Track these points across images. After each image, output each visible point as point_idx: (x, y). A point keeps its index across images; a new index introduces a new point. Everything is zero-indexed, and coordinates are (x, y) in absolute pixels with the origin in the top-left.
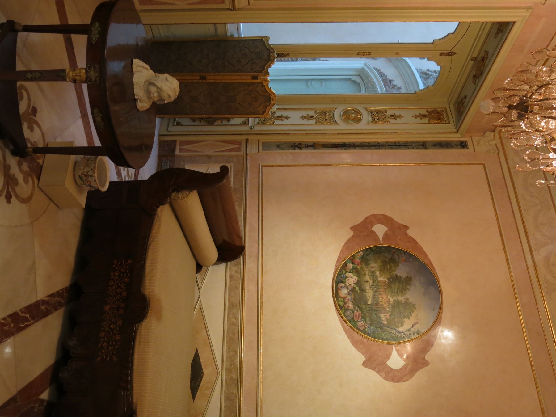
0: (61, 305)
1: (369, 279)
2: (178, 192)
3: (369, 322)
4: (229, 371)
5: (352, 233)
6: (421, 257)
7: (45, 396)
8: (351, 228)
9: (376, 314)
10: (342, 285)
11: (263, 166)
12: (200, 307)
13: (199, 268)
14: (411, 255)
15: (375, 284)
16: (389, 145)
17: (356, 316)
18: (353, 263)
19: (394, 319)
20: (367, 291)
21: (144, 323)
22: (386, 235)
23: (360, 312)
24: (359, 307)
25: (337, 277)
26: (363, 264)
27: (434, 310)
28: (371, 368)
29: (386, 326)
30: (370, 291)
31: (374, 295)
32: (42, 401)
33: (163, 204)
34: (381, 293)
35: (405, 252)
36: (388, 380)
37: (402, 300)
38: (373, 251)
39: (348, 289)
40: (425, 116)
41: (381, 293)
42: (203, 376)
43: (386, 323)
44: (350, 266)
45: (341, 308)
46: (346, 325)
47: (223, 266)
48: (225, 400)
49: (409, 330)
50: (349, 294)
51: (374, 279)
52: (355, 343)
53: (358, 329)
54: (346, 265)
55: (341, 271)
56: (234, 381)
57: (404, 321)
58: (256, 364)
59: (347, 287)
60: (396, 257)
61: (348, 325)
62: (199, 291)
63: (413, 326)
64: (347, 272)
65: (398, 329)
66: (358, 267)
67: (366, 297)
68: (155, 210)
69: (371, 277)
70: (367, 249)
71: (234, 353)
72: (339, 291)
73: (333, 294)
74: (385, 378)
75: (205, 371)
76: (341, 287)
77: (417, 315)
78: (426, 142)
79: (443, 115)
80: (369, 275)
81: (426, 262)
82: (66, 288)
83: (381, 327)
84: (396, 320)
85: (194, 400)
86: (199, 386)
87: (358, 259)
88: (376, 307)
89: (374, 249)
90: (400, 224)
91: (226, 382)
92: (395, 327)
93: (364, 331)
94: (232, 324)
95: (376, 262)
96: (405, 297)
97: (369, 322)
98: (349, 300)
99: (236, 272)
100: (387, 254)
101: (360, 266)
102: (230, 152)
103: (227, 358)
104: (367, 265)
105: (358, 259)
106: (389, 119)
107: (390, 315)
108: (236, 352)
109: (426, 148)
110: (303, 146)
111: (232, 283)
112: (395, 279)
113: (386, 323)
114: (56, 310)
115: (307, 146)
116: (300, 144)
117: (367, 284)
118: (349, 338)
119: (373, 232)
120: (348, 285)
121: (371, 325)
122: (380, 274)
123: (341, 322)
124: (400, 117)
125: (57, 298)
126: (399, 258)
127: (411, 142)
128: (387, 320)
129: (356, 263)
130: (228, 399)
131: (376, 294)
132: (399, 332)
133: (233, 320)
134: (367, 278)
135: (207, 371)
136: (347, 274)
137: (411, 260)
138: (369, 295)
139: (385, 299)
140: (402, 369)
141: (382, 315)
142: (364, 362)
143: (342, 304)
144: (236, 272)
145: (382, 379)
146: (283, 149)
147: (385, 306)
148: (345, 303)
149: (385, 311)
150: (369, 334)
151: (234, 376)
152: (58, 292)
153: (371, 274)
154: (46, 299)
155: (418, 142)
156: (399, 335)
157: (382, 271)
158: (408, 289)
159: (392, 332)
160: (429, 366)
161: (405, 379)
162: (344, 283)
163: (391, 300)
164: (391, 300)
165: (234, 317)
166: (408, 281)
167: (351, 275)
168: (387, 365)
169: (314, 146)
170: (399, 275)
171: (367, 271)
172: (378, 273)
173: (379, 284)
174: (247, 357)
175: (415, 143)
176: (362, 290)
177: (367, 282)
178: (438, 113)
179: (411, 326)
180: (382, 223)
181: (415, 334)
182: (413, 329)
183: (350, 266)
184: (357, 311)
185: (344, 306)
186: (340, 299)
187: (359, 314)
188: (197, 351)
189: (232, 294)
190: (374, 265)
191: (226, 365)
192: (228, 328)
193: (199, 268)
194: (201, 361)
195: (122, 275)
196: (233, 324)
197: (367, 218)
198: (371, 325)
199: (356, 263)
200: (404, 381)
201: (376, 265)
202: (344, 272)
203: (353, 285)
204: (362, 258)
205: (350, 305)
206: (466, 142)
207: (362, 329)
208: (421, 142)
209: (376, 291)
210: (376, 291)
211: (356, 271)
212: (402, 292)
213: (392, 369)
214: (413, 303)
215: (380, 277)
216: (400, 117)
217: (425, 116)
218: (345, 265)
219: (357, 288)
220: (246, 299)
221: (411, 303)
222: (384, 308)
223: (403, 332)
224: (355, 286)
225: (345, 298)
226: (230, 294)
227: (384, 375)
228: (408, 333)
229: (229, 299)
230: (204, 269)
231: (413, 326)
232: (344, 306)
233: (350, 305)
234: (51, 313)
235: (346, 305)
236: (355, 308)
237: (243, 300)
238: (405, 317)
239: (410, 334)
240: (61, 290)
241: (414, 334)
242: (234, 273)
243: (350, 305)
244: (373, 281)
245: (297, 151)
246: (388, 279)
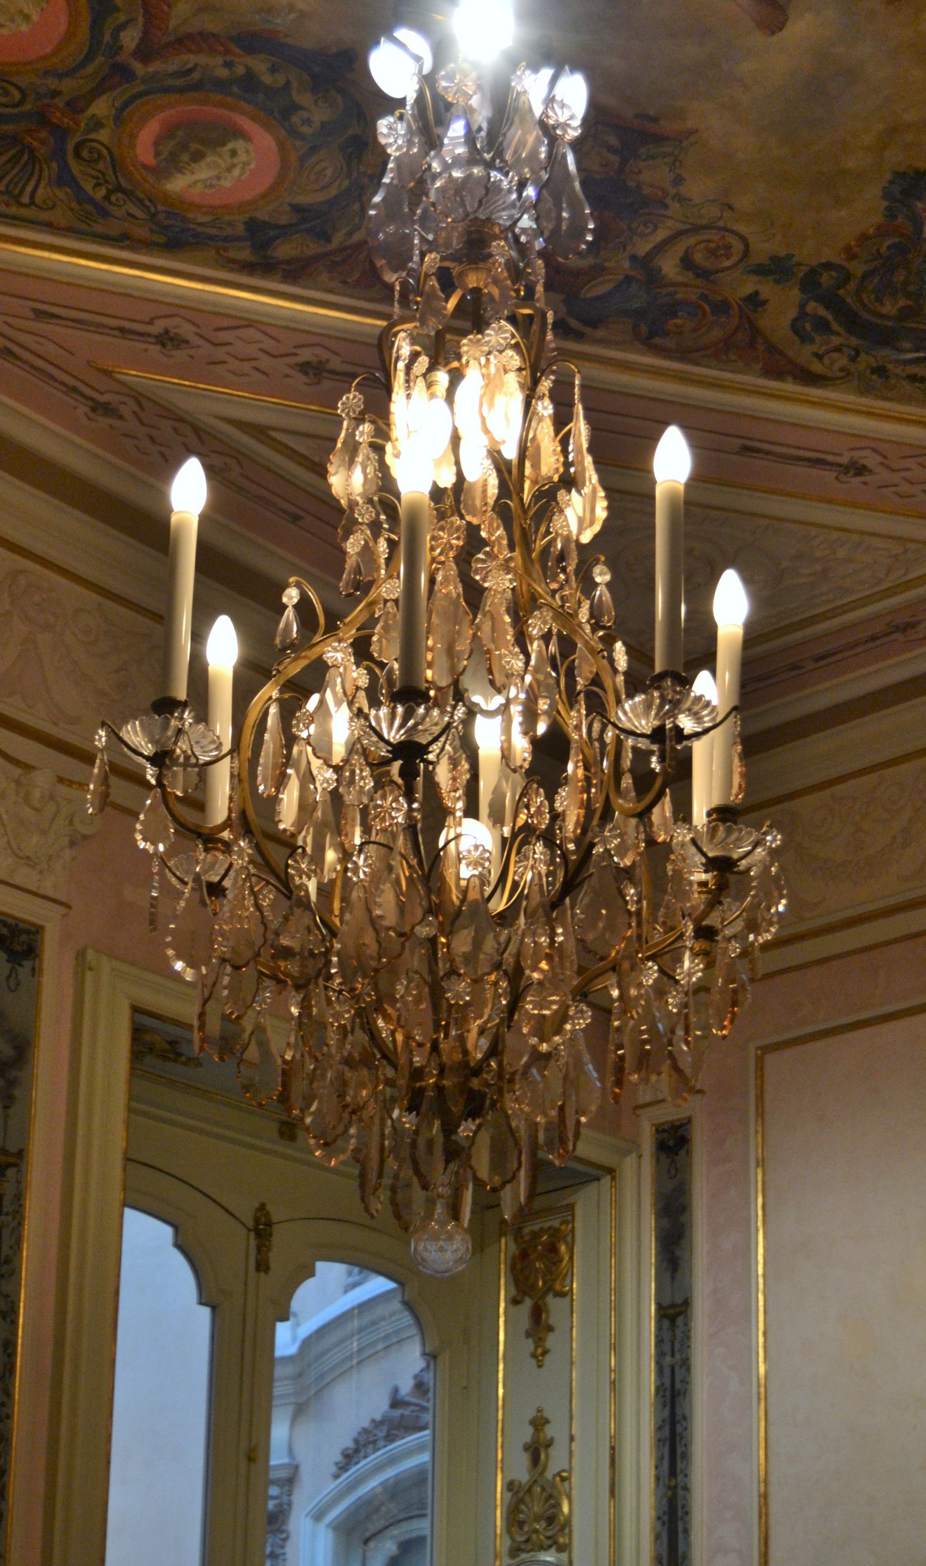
16: (673, 1472)
40: (538, 1313)
78: (659, 1307)
79: (536, 1235)
106: (549, 1475)
124: (539, 1423)
155: (659, 1342)
175: (660, 1355)
178: (524, 1255)
208: (659, 1329)
216: (539, 1423)
217: (538, 1313)
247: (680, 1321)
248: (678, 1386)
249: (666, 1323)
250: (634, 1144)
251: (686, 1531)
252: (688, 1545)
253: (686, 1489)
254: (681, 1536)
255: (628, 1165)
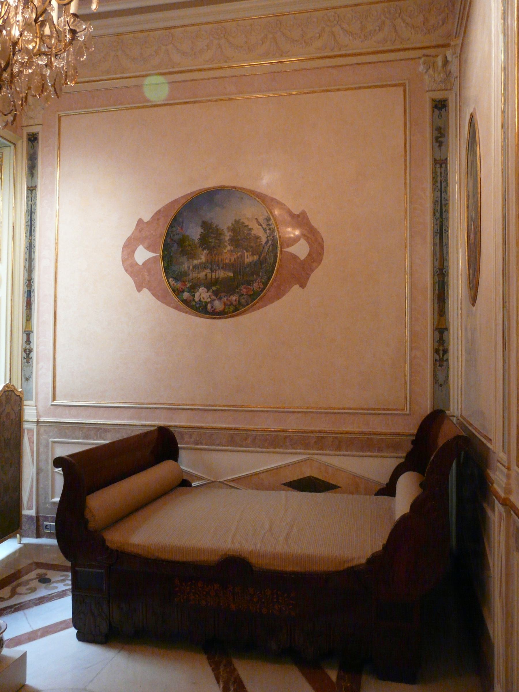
0: (229, 664)
1: (204, 273)
2: (86, 522)
3: (255, 276)
4: (307, 446)
5: (145, 290)
6: (178, 207)
7: (333, 675)
8: (139, 291)
9: (245, 268)
10: (209, 306)
11: (54, 399)
12: (233, 480)
13: (185, 483)
14: (175, 219)
15: (210, 266)
16: (31, 235)
17: (247, 292)
18: (183, 292)
19: (252, 247)
20: (217, 276)
21: (254, 561)
22: (148, 248)
23: (242, 287)
24: (237, 287)
25: (199, 312)
26: (184, 279)
27: (242, 198)
28: (308, 278)
29: (260, 256)
30: (217, 273)
31: (222, 268)
32: (339, 677)
33: (104, 541)
34: (220, 259)
35: (171, 226)
36: (321, 260)
37: (230, 236)
38: (168, 266)
39: (215, 300)
41: (220, 259)
42: (313, 477)
43: (256, 257)
44: (186, 295)
45: (236, 310)
46: (257, 305)
47: (183, 455)
48: (340, 450)
49: (265, 230)
50: (220, 299)
51: (202, 267)
52: (278, 296)
53: (262, 291)
54: (186, 300)
55: (192, 307)
56: (320, 441)
57: (254, 234)
58: (300, 415)
59: (212, 301)
60: (177, 237)
61: (257, 302)
62: (213, 482)
63: (261, 225)
64: (194, 300)
65: (263, 243)
66: (188, 285)
67: (223, 278)
68: (112, 550)
69: (200, 270)
70: (166, 273)
71: (287, 440)
72: (217, 310)
73: (220, 318)
74: (320, 262)
75: (307, 474)
76: (212, 307)
77: (248, 219)
78: (28, 187)
80: (198, 273)
81: (183, 201)
82: (208, 659)
83: (261, 263)
84: (252, 244)
85: (339, 487)
86: (323, 482)
87: (179, 285)
88: (237, 268)
89: (166, 265)
90: (136, 228)
91: (320, 450)
92: (262, 247)
93: (265, 284)
94: (254, 443)
95: (183, 263)
96: (226, 231)
97: (255, 276)
98: (227, 300)
99: (191, 437)
100: (173, 249)
101: (186, 283)
102: (33, 443)
103: (293, 448)
104: (186, 274)
105: (179, 285)
107: (247, 251)
108: (286, 437)
109: (36, 187)
110: (28, 347)
111: (204, 442)
112: (204, 241)
113: (256, 257)
114: (235, 670)
115: (28, 341)
116: (25, 351)
117: (209, 276)
118: (273, 302)
119: (144, 264)
120: (209, 300)
121: (258, 274)
122: (196, 259)
123: (254, 310)
125: (221, 670)
126: (178, 234)
127: (27, 205)
128: (253, 254)
129: (183, 287)
130: (339, 448)
131: (221, 266)
132: (267, 242)
133: (249, 441)
134: (202, 275)
135: (307, 472)
136: (197, 299)
137: (181, 220)
138: (222, 274)
139: (228, 256)
140: (309, 243)
141: (247, 261)
142: (300, 286)
143: (232, 308)
144: (191, 437)
145: (320, 267)
146: (32, 373)
147: (235, 256)
148: (232, 304)
149: (242, 256)
150: (269, 279)
151: (313, 441)
152: (213, 670)
153: (197, 270)
154: (221, 686)
155: (27, 197)
156: (270, 242)
157: (193, 256)
158: (216, 226)
159: (266, 250)
160: (306, 210)
161: (320, 240)
162: (207, 304)
163: (229, 248)
164: (229, 248)
165: (246, 440)
166: (206, 225)
167: (197, 295)
168: (304, 260)
169: (28, 334)
170: (199, 237)
171: (193, 275)
172: (196, 262)
173: (209, 261)
174: (293, 424)
175: (28, 201)
176: (216, 282)
177: (206, 275)
179: (260, 227)
180: (134, 251)
181: (270, 223)
182: (264, 226)
183: (186, 295)
184: (241, 290)
185: (235, 306)
186: (226, 310)
187: (245, 288)
188: (284, 484)
189: (218, 442)
190: (186, 265)
191: (300, 449)
192: (259, 447)
193: (185, 483)
194: (295, 479)
195: (193, 591)
196: (254, 440)
197: (126, 271)
198: (258, 274)
199: (183, 287)
200: (323, 241)
201: (186, 263)
202: (194, 303)
203: (210, 293)
204: (176, 279)
205: (234, 298)
206: (29, 135)
207: (262, 287)
208: (27, 193)
209: (218, 265)
210: (218, 265)
211: (193, 289)
212: (220, 234)
213: (309, 254)
214: (233, 223)
215: (201, 259)
218: (186, 302)
219: (214, 288)
220: (224, 426)
221: (232, 224)
222: (238, 258)
223: (267, 238)
224: (211, 290)
225: (225, 304)
226: (218, 445)
227: (315, 264)
228: (268, 231)
229: (224, 446)
230: (185, 478)
231: (261, 225)
232: (235, 306)
233: (234, 298)
234: (238, 676)
235: (234, 303)
236: (238, 292)
237: (225, 429)
238: (249, 234)
239: (270, 229)
240: (211, 666)
241: (269, 225)
242: (193, 440)
243: (234, 298)
244: (205, 268)
245: (34, 354)
246: (204, 249)
247: (34, 191)
248: (33, 210)
249: (30, 192)
250: (22, 137)
251: (34, 252)
252: (34, 256)
253: (34, 240)
254: (32, 253)
255: (19, 143)
